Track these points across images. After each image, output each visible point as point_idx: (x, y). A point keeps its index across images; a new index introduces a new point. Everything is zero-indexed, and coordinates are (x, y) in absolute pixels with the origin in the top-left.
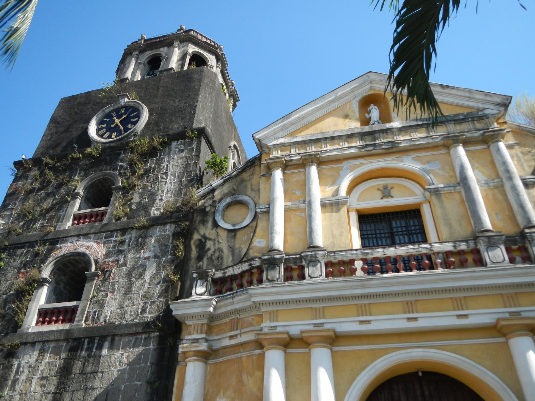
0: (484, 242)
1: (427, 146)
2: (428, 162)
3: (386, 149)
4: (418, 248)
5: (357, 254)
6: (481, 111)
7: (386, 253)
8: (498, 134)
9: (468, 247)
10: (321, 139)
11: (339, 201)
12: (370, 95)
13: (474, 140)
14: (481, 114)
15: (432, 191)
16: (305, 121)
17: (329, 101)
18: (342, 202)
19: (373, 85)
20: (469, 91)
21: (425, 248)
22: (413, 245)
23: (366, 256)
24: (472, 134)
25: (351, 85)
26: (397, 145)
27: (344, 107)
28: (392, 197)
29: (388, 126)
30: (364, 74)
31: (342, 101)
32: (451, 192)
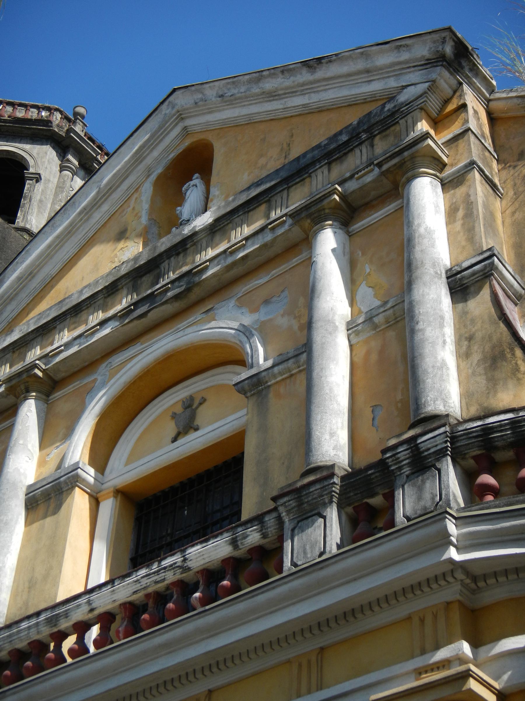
0: (288, 512)
1: (270, 253)
2: (267, 302)
3: (176, 297)
4: (157, 572)
5: (37, 624)
6: (391, 98)
7: (94, 605)
8: (413, 157)
9: (264, 536)
10: (55, 319)
11: (59, 483)
12: (184, 151)
13: (373, 194)
14: (389, 110)
15: (247, 388)
16: (36, 283)
17: (85, 208)
18: (65, 482)
19: (188, 122)
20: (362, 53)
21: (172, 567)
22: (148, 566)
23: (55, 625)
24: (361, 181)
25: (134, 145)
26: (197, 279)
27: (124, 210)
28: (197, 429)
29: (187, 230)
30: (162, 103)
31: (116, 195)
32: (292, 375)
